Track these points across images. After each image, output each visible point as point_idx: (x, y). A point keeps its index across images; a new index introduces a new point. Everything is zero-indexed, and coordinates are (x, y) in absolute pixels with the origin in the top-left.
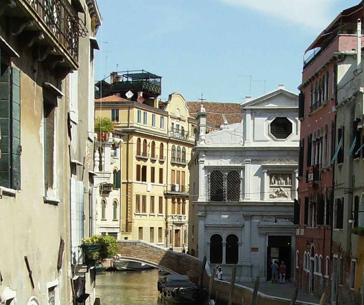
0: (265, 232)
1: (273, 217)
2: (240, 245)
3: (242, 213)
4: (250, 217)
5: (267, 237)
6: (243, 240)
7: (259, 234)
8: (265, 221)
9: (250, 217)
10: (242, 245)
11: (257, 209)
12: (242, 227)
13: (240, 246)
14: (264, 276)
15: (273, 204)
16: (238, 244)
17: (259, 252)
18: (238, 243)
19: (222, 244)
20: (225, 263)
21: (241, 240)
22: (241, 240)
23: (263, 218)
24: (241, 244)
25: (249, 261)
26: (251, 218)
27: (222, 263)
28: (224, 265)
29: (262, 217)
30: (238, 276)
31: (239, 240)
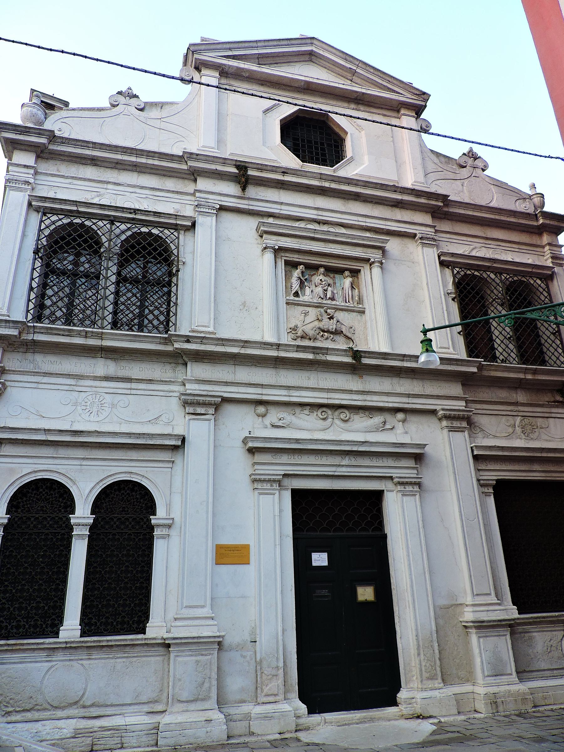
0: (283, 473)
1: (307, 412)
2: (165, 531)
4: (209, 404)
5: (287, 497)
6: (176, 514)
7: (254, 481)
8: (273, 426)
9: (209, 404)
10: (173, 532)
12: (175, 448)
13: (163, 537)
14: (281, 697)
15: (310, 356)
16: (152, 528)
17: (249, 571)
18: (154, 521)
19: (70, 528)
20: (78, 633)
21: (168, 512)
22: (168, 512)
23: (264, 416)
24: (169, 526)
25: (206, 612)
26: (217, 407)
27: (56, 634)
28: (69, 647)
29: (261, 409)
30: (146, 708)
31: (161, 511)
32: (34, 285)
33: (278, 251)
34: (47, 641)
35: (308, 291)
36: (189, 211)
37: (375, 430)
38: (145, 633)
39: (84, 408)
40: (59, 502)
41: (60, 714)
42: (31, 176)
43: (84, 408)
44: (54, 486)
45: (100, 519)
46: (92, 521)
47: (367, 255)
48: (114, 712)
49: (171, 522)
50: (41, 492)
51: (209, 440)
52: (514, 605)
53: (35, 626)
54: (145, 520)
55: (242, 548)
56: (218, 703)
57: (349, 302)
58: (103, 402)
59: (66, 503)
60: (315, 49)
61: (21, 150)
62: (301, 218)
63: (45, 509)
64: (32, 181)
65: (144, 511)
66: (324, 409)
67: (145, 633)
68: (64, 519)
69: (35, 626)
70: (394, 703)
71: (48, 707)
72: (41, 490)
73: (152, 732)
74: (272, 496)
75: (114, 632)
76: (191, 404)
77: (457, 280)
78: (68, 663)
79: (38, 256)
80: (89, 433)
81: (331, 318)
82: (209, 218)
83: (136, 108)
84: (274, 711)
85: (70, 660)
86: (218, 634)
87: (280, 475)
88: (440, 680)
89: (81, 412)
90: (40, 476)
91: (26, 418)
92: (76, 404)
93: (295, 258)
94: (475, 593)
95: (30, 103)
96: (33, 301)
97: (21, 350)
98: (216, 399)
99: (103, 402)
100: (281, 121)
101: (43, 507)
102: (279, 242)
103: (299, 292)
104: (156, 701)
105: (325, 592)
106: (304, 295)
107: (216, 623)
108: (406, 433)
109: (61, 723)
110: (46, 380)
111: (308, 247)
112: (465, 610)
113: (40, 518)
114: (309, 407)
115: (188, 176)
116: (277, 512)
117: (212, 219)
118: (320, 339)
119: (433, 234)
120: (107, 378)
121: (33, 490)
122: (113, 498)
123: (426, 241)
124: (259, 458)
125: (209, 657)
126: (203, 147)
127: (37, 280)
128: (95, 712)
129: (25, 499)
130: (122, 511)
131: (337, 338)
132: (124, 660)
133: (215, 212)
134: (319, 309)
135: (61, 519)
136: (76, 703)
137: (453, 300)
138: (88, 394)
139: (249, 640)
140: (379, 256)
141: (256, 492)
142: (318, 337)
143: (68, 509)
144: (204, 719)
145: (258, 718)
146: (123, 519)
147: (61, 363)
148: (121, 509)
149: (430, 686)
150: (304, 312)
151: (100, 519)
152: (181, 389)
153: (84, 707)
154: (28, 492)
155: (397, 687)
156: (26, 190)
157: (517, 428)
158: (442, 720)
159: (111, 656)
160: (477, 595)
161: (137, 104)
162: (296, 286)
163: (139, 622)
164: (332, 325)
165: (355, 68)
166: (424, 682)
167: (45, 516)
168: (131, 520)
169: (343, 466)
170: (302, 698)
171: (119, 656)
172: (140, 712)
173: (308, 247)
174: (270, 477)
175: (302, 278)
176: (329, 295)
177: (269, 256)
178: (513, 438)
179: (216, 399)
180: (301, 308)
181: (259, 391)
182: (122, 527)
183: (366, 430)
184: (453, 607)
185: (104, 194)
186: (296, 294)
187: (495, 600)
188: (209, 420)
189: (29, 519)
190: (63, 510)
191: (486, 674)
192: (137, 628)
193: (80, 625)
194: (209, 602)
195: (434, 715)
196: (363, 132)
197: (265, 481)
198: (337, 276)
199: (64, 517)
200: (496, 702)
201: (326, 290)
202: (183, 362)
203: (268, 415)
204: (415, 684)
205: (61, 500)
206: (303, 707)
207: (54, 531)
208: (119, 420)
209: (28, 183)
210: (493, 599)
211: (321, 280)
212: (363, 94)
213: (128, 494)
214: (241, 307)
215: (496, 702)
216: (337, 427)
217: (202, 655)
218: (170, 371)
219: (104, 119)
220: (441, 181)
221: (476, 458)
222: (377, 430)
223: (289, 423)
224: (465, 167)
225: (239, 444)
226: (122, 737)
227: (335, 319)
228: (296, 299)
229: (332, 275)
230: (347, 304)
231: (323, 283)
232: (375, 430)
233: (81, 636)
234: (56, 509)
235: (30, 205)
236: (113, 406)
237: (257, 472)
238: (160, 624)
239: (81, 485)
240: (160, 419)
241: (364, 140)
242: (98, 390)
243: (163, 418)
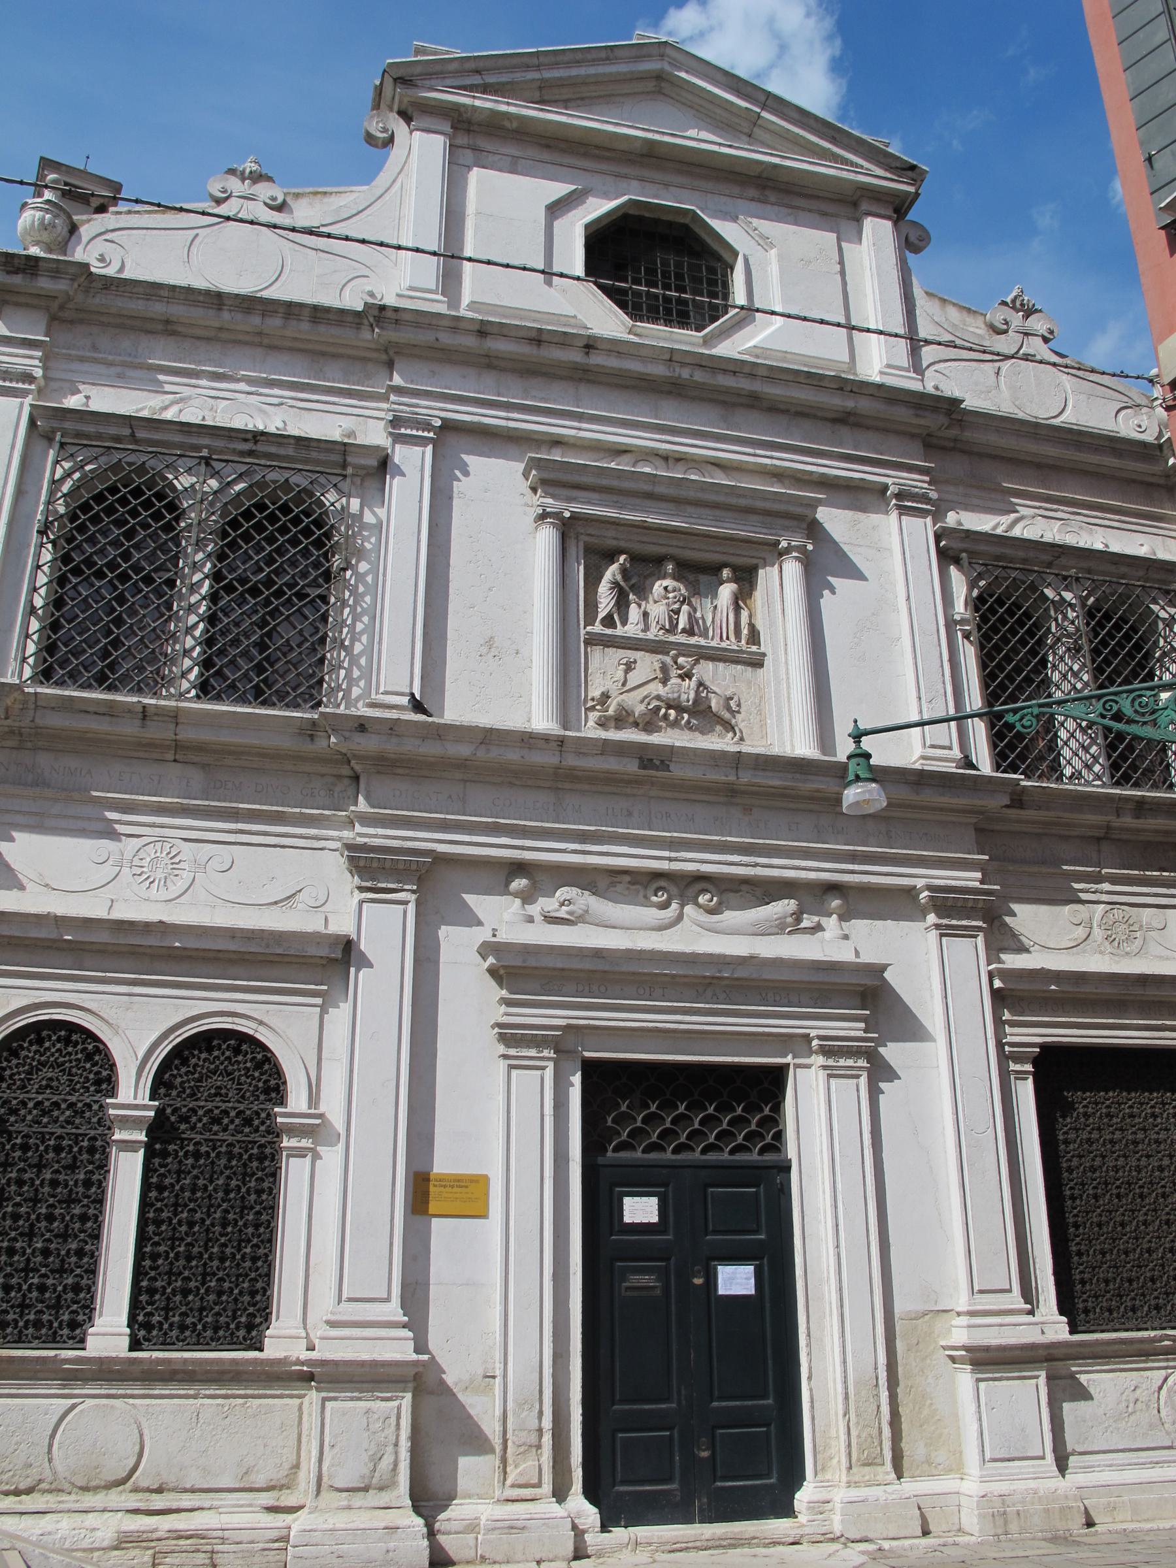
13: (300, 1153)
14: (547, 1488)
16: (275, 1133)
19: (105, 1125)
20: (126, 1342)
21: (314, 1097)
22: (314, 1097)
27: (81, 1342)
31: (297, 1099)
32: (39, 602)
35: (634, 613)
36: (375, 434)
37: (776, 930)
38: (261, 1350)
40: (85, 1070)
41: (90, 1500)
42: (36, 362)
43: (139, 871)
44: (74, 1037)
45: (169, 1111)
46: (152, 1114)
48: (197, 1504)
49: (318, 1121)
52: (1061, 1314)
53: (38, 1324)
54: (263, 1115)
55: (472, 1181)
56: (414, 1497)
57: (728, 638)
60: (667, 67)
61: (17, 304)
62: (624, 448)
63: (55, 1084)
64: (38, 373)
66: (662, 883)
67: (261, 1350)
68: (95, 1107)
69: (38, 1324)
70: (786, 1510)
72: (47, 1044)
73: (276, 1545)
75: (198, 1344)
77: (975, 593)
79: (48, 538)
81: (688, 675)
82: (418, 450)
83: (266, 204)
84: (528, 1516)
88: (889, 1466)
93: (610, 539)
94: (976, 1288)
95: (40, 200)
96: (35, 637)
97: (9, 743)
99: (176, 860)
100: (587, 227)
101: (51, 1079)
103: (616, 617)
104: (282, 1487)
105: (647, 1280)
106: (624, 622)
108: (846, 937)
109: (91, 1520)
112: (954, 1323)
114: (627, 878)
115: (374, 355)
119: (926, 485)
123: (908, 505)
125: (396, 1403)
126: (411, 289)
127: (43, 591)
128: (158, 1502)
129: (15, 1062)
130: (216, 1095)
132: (219, 1401)
135: (89, 1106)
136: (123, 1481)
137: (967, 636)
139: (480, 1372)
143: (104, 1086)
144: (383, 1525)
145: (495, 1529)
147: (89, 772)
148: (213, 1091)
149: (867, 1478)
150: (624, 661)
151: (169, 1111)
153: (136, 1490)
154: (22, 1048)
155: (793, 1476)
156: (23, 394)
157: (1096, 930)
158: (886, 1545)
159: (191, 1392)
160: (981, 1292)
161: (270, 194)
163: (250, 1327)
164: (687, 691)
165: (758, 110)
166: (854, 1470)
167: (55, 1098)
168: (233, 1114)
170: (592, 1493)
171: (207, 1392)
172: (251, 1505)
175: (622, 583)
176: (683, 622)
178: (1084, 952)
182: (215, 1128)
183: (754, 929)
184: (927, 1317)
185: (190, 398)
187: (1019, 1303)
189: (24, 1104)
190: (92, 1089)
191: (988, 1456)
192: (245, 1339)
193: (129, 1326)
195: (871, 1535)
196: (773, 252)
198: (703, 578)
199: (95, 1102)
200: (1005, 1513)
201: (678, 612)
202: (350, 773)
204: (837, 1471)
206: (590, 1514)
207: (74, 1131)
209: (28, 378)
210: (1015, 1300)
211: (666, 588)
212: (776, 166)
213: (228, 1058)
214: (484, 650)
215: (1005, 1513)
218: (322, 793)
219: (196, 231)
220: (949, 364)
221: (996, 994)
222: (780, 928)
223: (581, 912)
224: (1006, 332)
226: (213, 1552)
227: (694, 679)
228: (609, 631)
229: (691, 577)
230: (724, 645)
232: (776, 930)
233: (131, 1349)
234: (78, 1086)
235: (32, 422)
238: (293, 1332)
241: (774, 269)
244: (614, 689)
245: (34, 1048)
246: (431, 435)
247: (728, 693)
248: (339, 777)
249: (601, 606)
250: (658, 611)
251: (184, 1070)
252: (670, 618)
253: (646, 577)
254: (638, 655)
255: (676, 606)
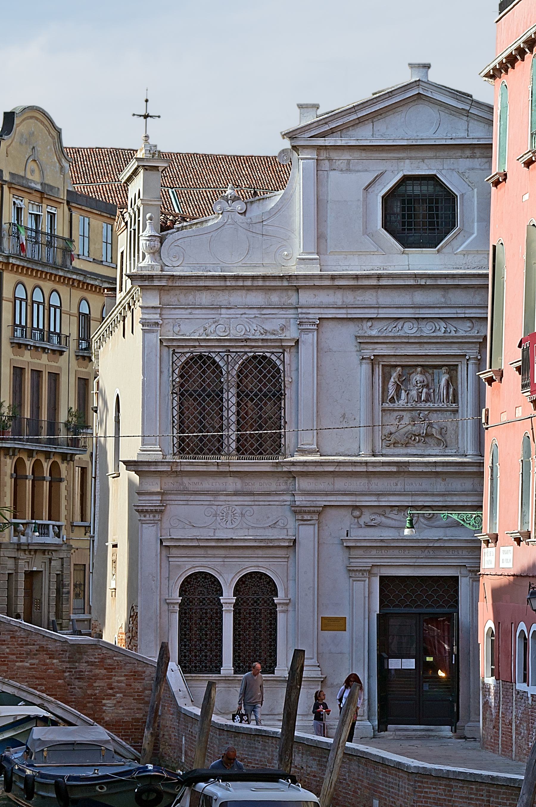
1: (395, 512)
3: (288, 498)
5: (376, 582)
9: (314, 512)
11: (341, 484)
14: (366, 717)
15: (394, 469)
26: (319, 513)
29: (357, 513)
33: (374, 361)
34: (214, 675)
35: (403, 395)
39: (222, 518)
43: (222, 518)
46: (235, 601)
47: (463, 351)
49: (288, 601)
50: (199, 581)
51: (314, 541)
54: (270, 599)
58: (234, 513)
59: (216, 588)
65: (270, 594)
71: (219, 713)
74: (363, 582)
76: (300, 512)
78: (228, 689)
80: (227, 540)
85: (229, 687)
86: (320, 676)
87: (369, 566)
89: (220, 521)
90: (197, 570)
91: (183, 528)
92: (216, 515)
93: (393, 361)
98: (318, 509)
99: (234, 513)
102: (376, 351)
107: (320, 669)
110: (192, 498)
111: (403, 351)
113: (201, 599)
114: (397, 508)
116: (367, 595)
117: (313, 335)
118: (412, 443)
120: (236, 493)
121: (194, 579)
122: (247, 584)
124: (354, 553)
129: (189, 586)
131: (428, 440)
133: (316, 327)
134: (413, 412)
138: (223, 507)
140: (475, 351)
141: (351, 579)
142: (410, 441)
146: (255, 599)
147: (201, 483)
150: (398, 417)
152: (292, 498)
162: (392, 391)
163: (270, 667)
167: (204, 597)
169: (422, 558)
173: (403, 351)
174: (361, 568)
175: (398, 382)
177: (366, 367)
179: (318, 509)
180: (396, 414)
181: (353, 498)
186: (392, 400)
188: (314, 525)
194: (316, 655)
197: (357, 571)
201: (421, 392)
203: (363, 516)
205: (213, 586)
208: (247, 526)
213: (258, 581)
214: (342, 419)
216: (421, 524)
217: (311, 688)
218: (283, 484)
225: (337, 541)
230: (441, 405)
231: (419, 385)
233: (234, 674)
236: (243, 515)
237: (352, 564)
238: (284, 668)
239: (225, 576)
240: (277, 524)
242: (230, 503)
243: (279, 523)
244: (393, 429)
245: (195, 581)
246: (316, 327)
247: (442, 426)
248: (289, 478)
249: (390, 391)
250: (414, 393)
251: (244, 586)
252: (418, 395)
253: (410, 374)
254: (404, 413)
255: (420, 390)
